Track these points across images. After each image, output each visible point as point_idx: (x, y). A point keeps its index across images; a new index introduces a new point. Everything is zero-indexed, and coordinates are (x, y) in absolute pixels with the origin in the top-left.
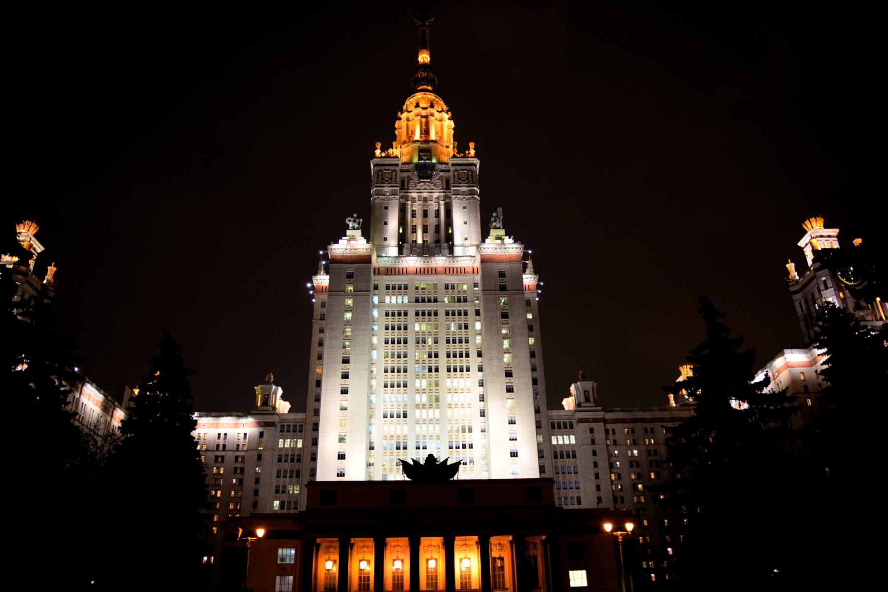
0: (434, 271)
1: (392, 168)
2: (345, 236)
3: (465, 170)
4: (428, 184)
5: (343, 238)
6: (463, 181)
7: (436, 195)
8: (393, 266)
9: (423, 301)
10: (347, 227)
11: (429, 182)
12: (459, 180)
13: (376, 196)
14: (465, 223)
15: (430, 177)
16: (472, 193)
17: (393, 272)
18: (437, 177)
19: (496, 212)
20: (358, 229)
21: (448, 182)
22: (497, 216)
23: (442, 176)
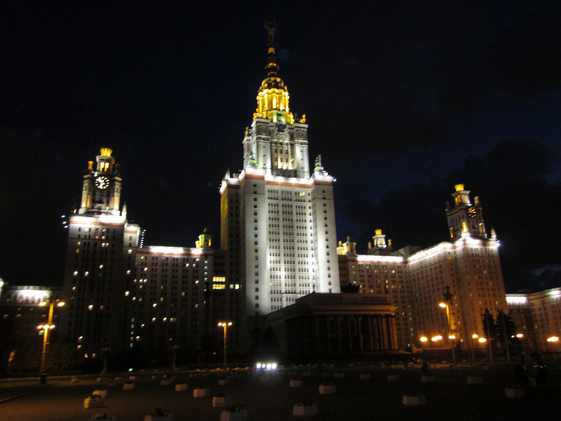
0: (290, 185)
7: (286, 142)
9: (285, 200)
12: (300, 136)
15: (283, 131)
16: (305, 144)
18: (286, 131)
22: (318, 159)
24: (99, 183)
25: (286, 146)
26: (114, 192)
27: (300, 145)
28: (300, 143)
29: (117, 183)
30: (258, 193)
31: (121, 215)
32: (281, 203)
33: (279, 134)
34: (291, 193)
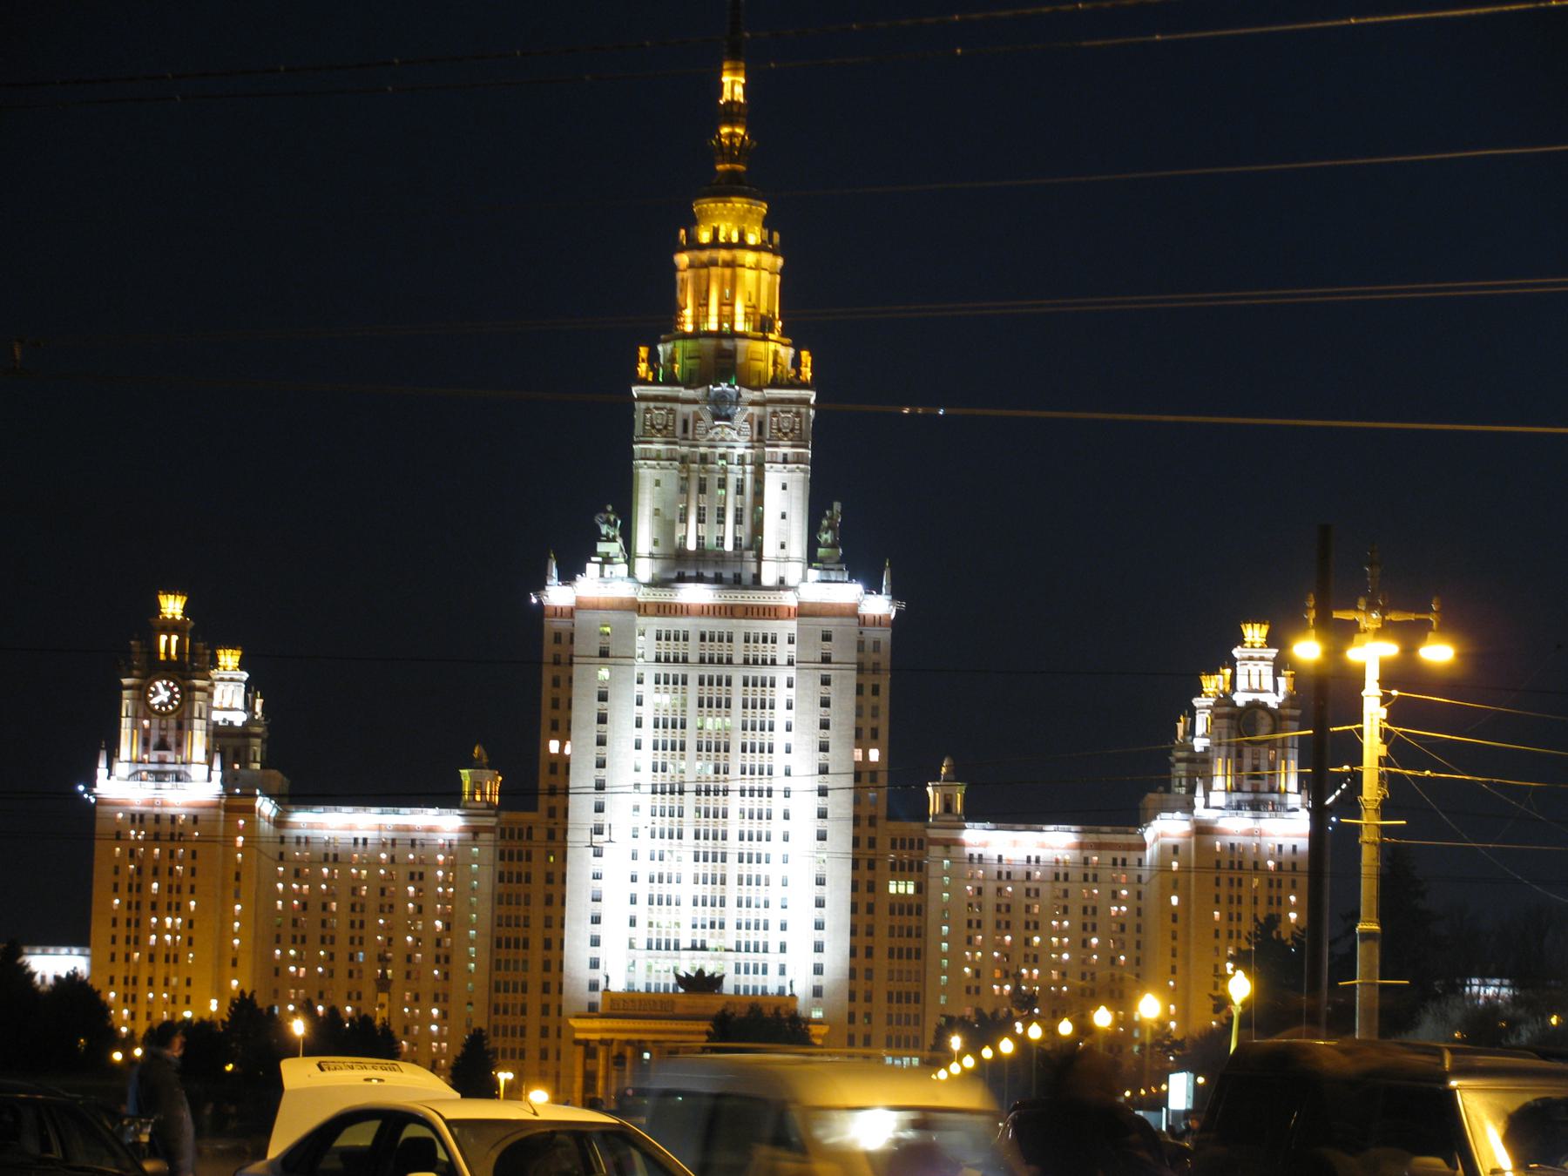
1: (668, 405)
2: (596, 554)
3: (789, 412)
4: (727, 430)
5: (593, 559)
6: (786, 434)
7: (739, 451)
8: (667, 601)
9: (711, 661)
10: (598, 537)
11: (727, 426)
12: (782, 434)
13: (642, 462)
14: (783, 516)
15: (728, 418)
16: (799, 460)
17: (667, 610)
18: (741, 416)
19: (831, 508)
20: (613, 540)
21: (761, 425)
22: (831, 518)
23: (753, 414)
24: (156, 693)
25: (735, 468)
26: (192, 718)
27: (781, 466)
28: (780, 459)
29: (198, 695)
30: (611, 653)
31: (209, 779)
32: (693, 674)
33: (711, 429)
34: (730, 640)
